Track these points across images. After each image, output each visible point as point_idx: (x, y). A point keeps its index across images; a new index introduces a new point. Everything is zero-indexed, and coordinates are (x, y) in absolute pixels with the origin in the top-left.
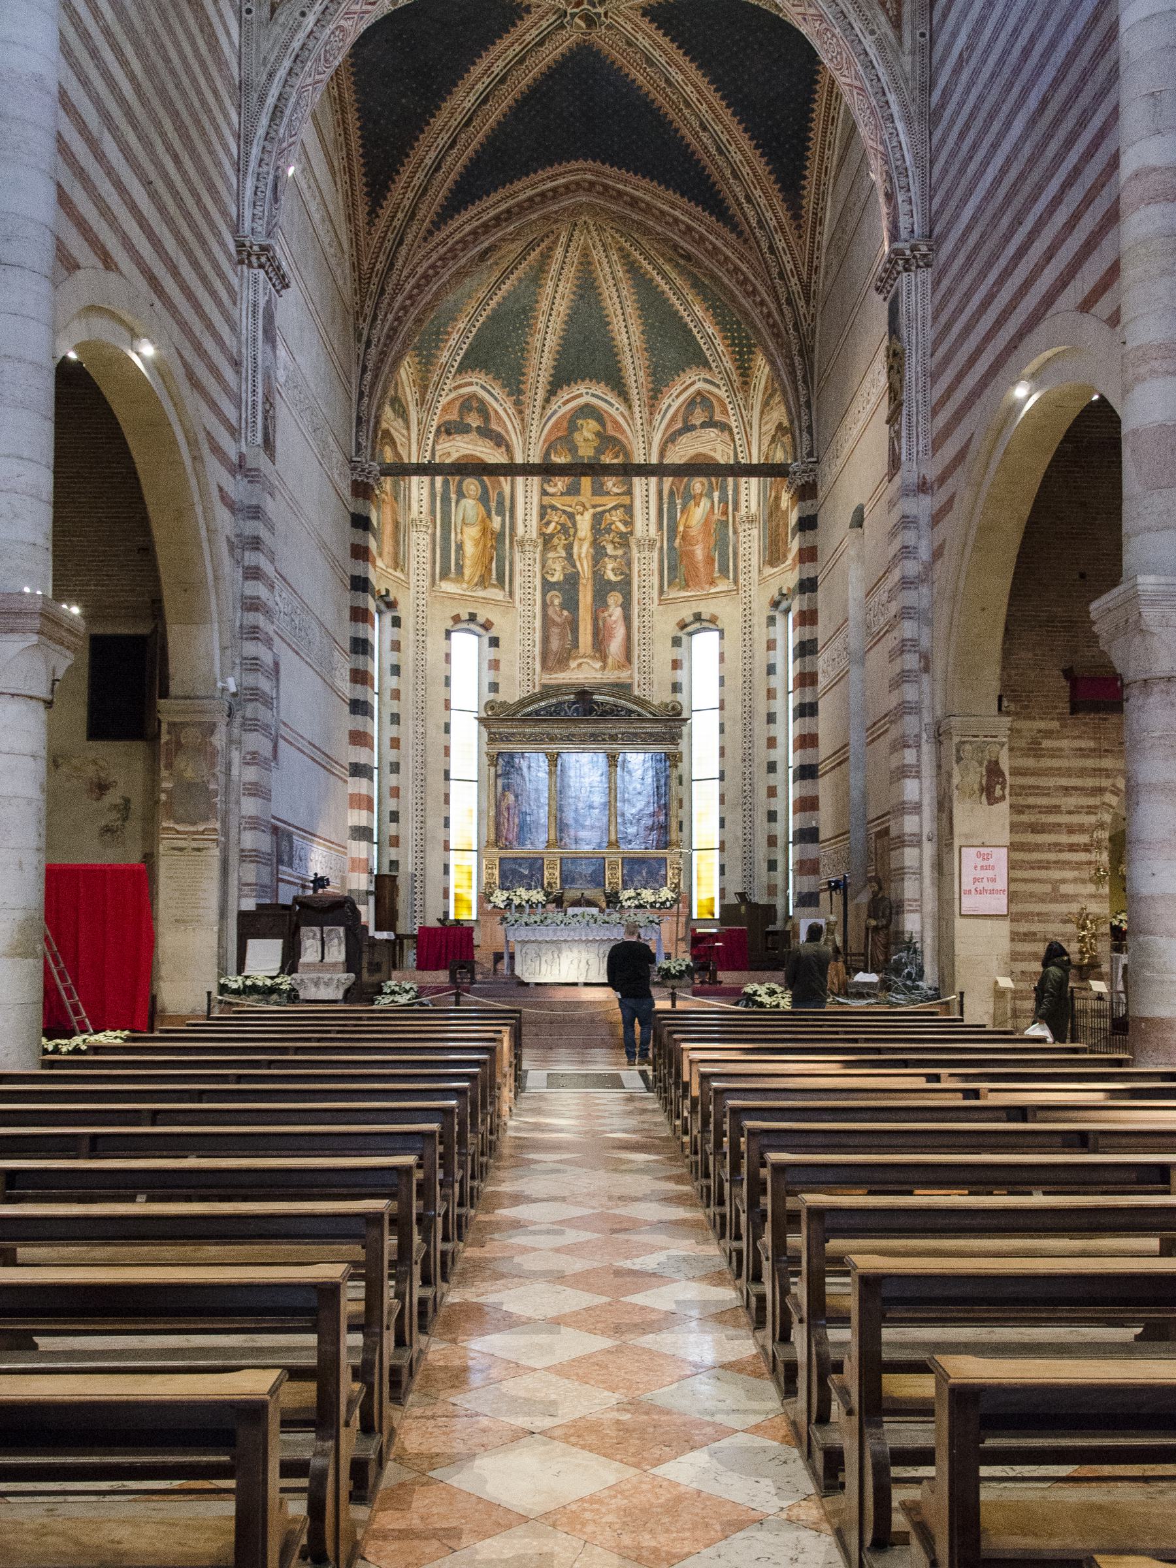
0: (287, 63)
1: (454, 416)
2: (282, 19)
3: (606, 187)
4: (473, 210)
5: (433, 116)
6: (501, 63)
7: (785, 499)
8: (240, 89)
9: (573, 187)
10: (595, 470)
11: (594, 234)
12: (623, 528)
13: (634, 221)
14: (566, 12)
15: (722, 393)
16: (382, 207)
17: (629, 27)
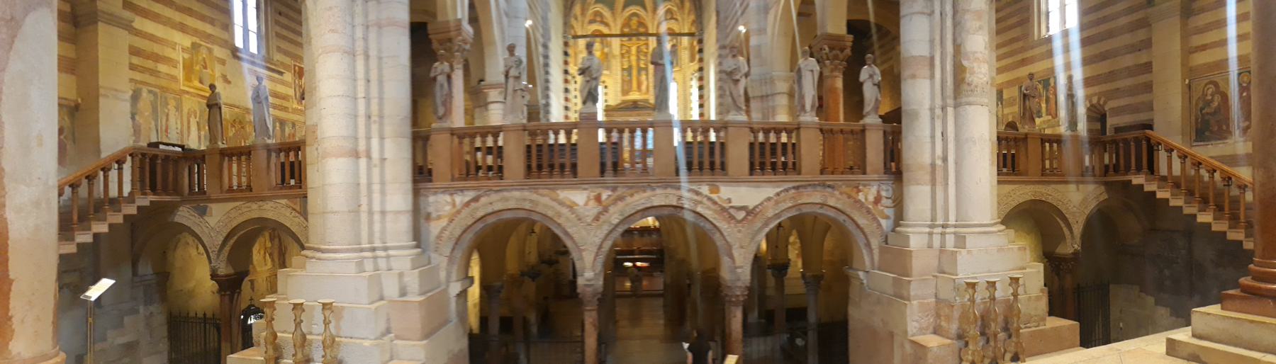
1: (592, 18)
7: (695, 43)
10: (638, 35)
12: (645, 50)
15: (675, 9)
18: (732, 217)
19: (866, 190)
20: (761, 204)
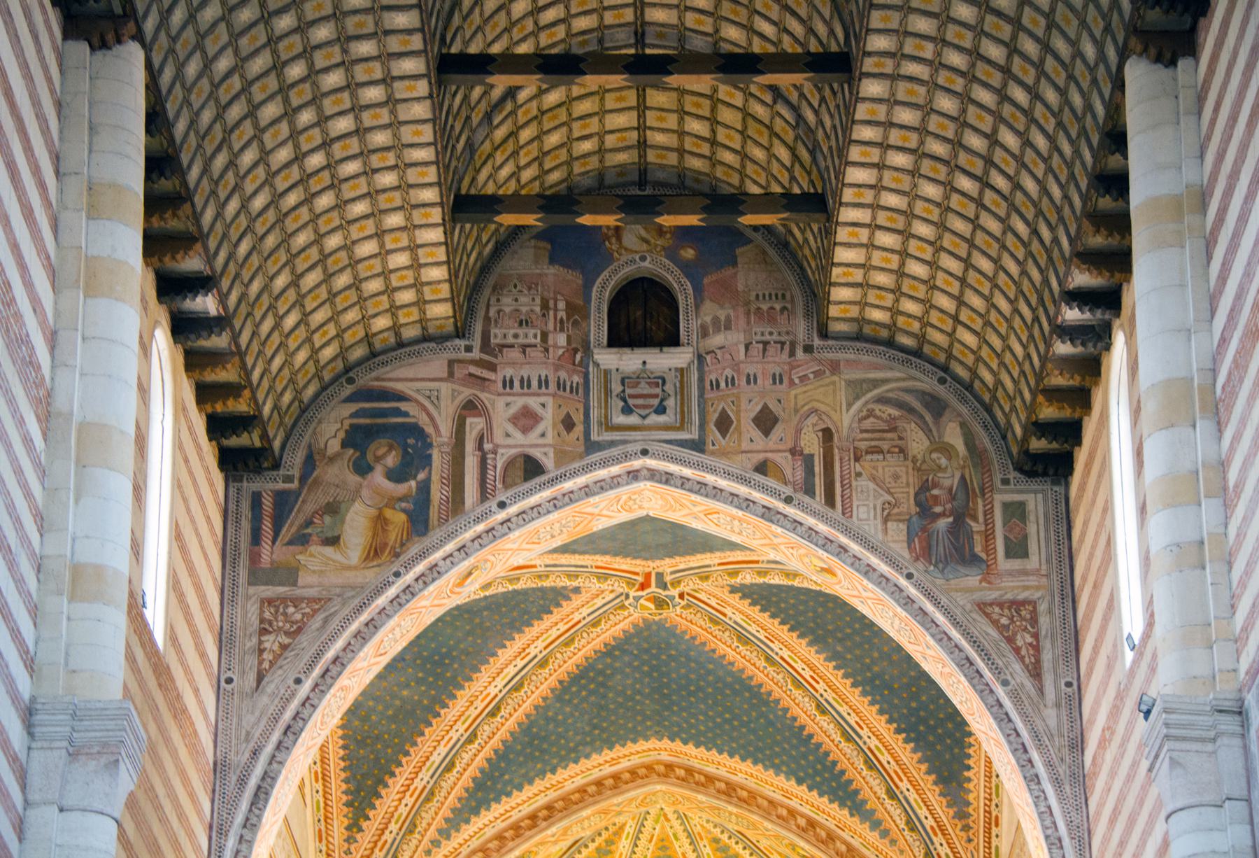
0: (275, 738)
2: (270, 688)
3: (690, 771)
4: (497, 809)
5: (446, 706)
6: (540, 644)
8: (215, 770)
9: (642, 771)
11: (676, 824)
13: (731, 814)
14: (627, 596)
16: (368, 818)
17: (713, 602)
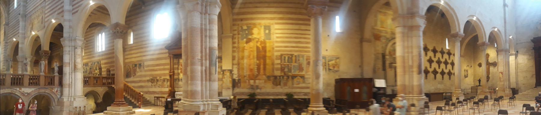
18: (24, 95)
19: (54, 89)
20: (31, 92)
